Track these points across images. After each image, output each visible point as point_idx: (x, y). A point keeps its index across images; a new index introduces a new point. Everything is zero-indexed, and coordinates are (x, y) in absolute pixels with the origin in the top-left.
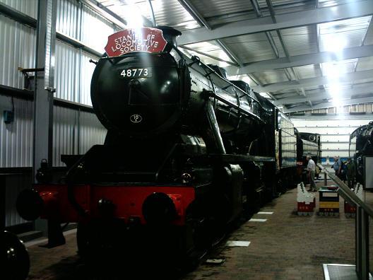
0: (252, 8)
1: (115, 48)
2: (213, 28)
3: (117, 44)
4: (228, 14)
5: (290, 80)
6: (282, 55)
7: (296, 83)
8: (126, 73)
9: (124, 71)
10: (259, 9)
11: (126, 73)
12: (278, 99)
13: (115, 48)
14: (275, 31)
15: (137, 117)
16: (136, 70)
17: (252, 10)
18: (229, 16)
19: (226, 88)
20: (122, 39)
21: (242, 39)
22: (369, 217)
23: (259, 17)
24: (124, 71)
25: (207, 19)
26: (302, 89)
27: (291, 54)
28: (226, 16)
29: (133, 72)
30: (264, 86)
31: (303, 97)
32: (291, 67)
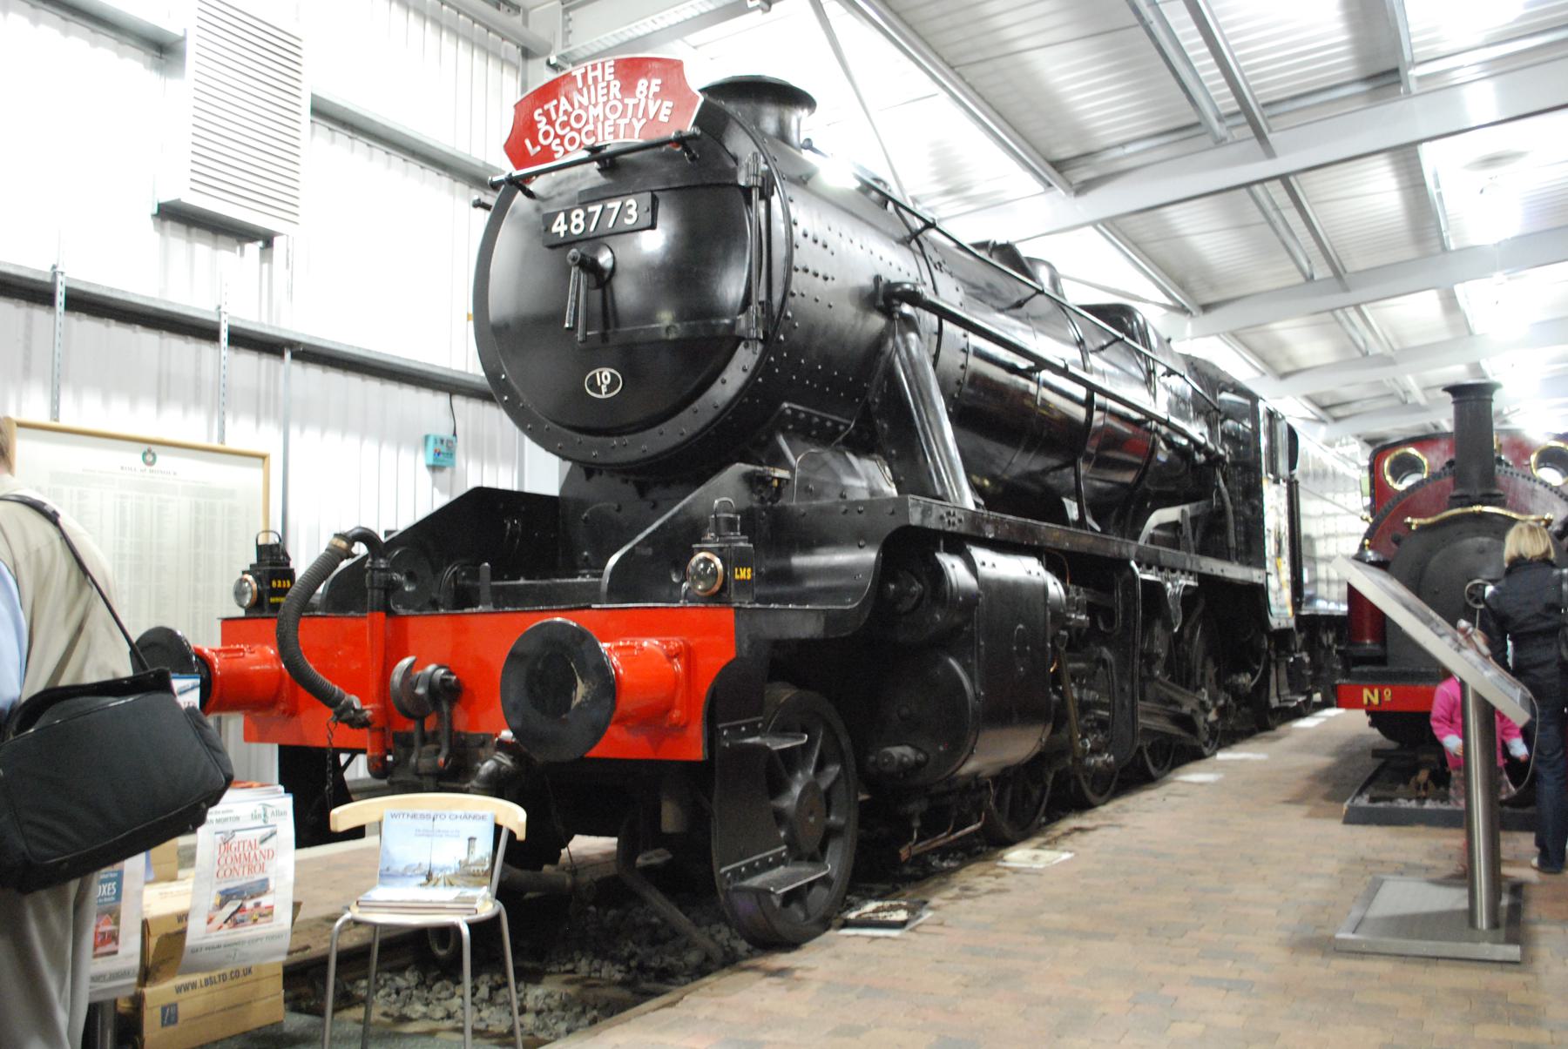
0: (1194, 119)
1: (535, 143)
2: (1082, 188)
3: (543, 127)
4: (1123, 145)
5: (1366, 354)
6: (1322, 272)
7: (1387, 361)
8: (568, 221)
9: (561, 217)
10: (1220, 119)
11: (568, 221)
12: (1336, 419)
13: (535, 143)
14: (1278, 184)
15: (605, 375)
16: (597, 208)
17: (1197, 124)
18: (1130, 149)
19: (1019, 305)
20: (557, 108)
21: (1180, 218)
22: (586, 756)
23: (1220, 142)
24: (561, 217)
25: (1059, 166)
26: (1411, 382)
27: (1354, 263)
28: (1118, 152)
29: (588, 217)
30: (1284, 376)
31: (1418, 408)
32: (1357, 307)
